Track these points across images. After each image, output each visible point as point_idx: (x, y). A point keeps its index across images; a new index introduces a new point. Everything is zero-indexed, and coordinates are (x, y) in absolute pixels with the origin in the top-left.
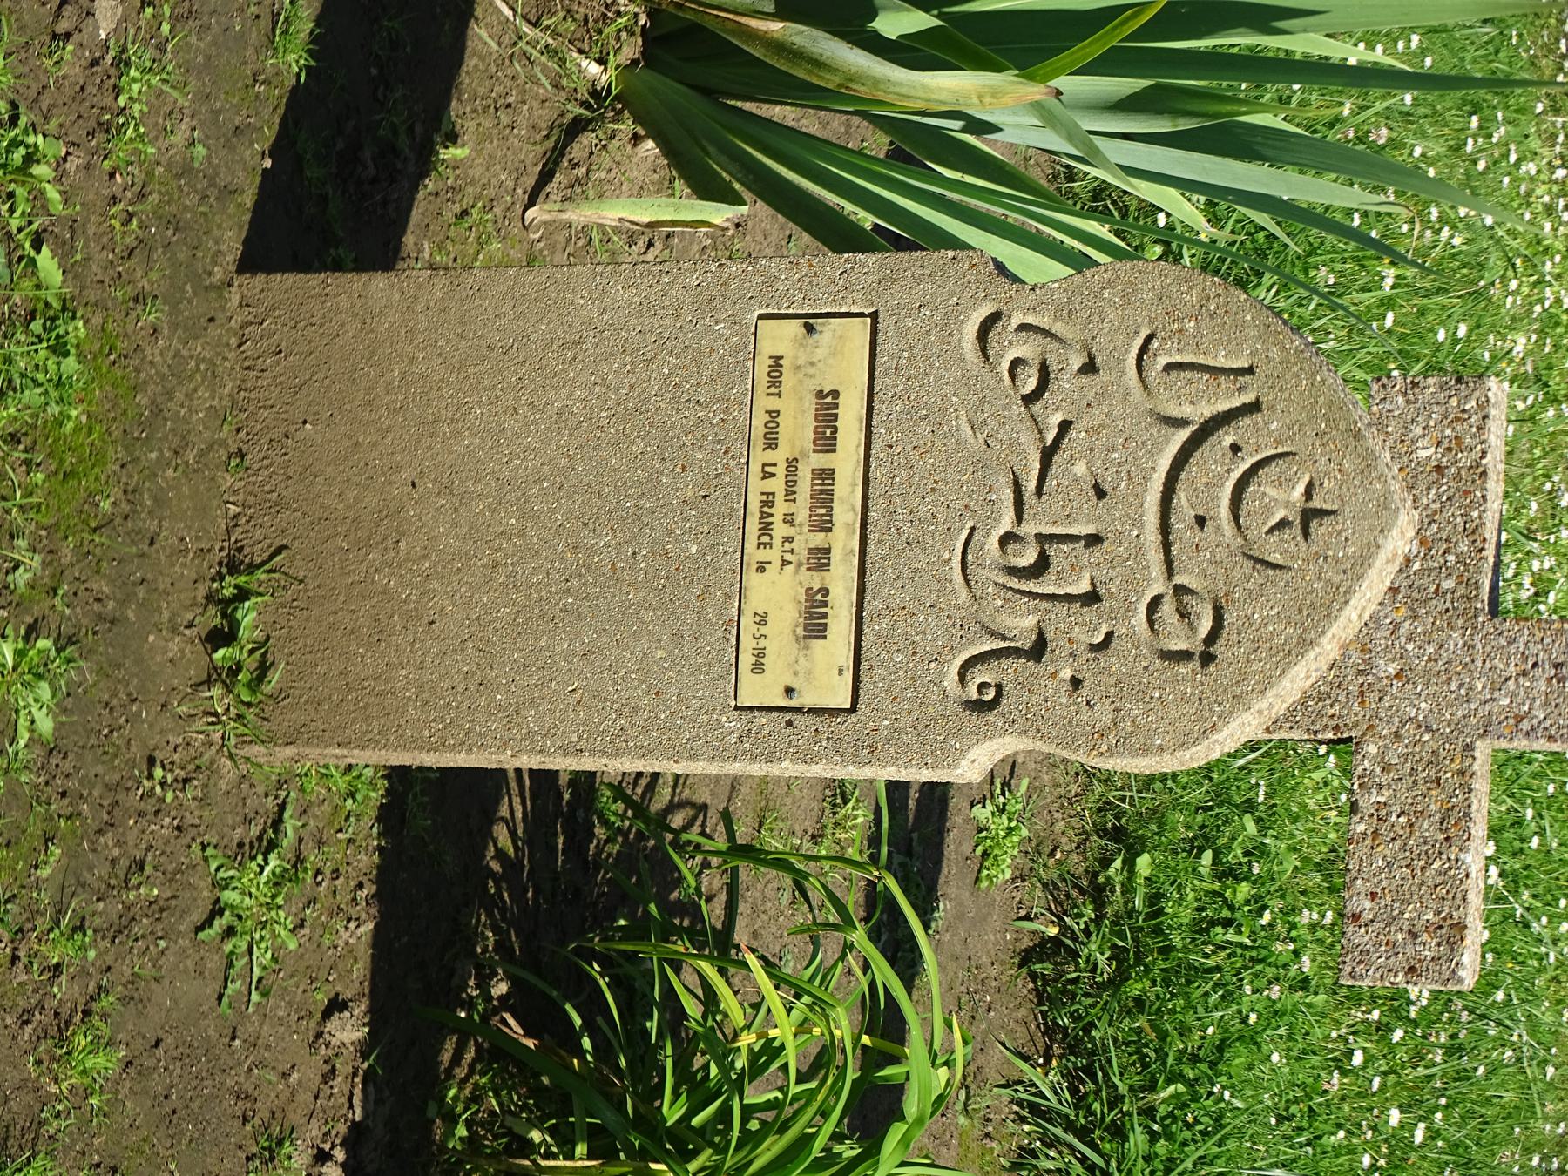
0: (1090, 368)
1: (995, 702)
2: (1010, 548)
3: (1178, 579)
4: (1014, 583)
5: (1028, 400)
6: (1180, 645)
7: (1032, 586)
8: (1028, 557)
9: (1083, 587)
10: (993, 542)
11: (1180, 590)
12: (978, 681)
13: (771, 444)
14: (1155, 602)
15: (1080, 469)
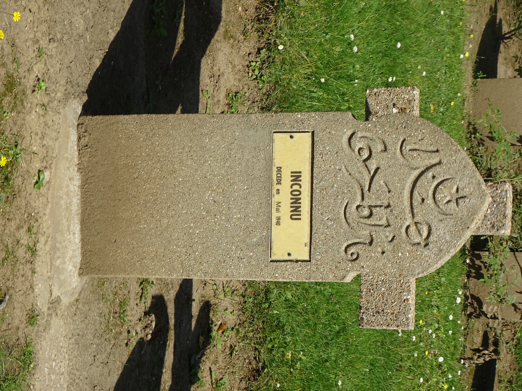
0: (385, 150)
1: (357, 259)
2: (360, 210)
3: (416, 219)
4: (362, 220)
5: (365, 161)
6: (417, 241)
7: (369, 222)
8: (366, 212)
9: (384, 222)
10: (354, 206)
11: (416, 223)
12: (351, 252)
13: (279, 183)
14: (408, 227)
15: (382, 182)
